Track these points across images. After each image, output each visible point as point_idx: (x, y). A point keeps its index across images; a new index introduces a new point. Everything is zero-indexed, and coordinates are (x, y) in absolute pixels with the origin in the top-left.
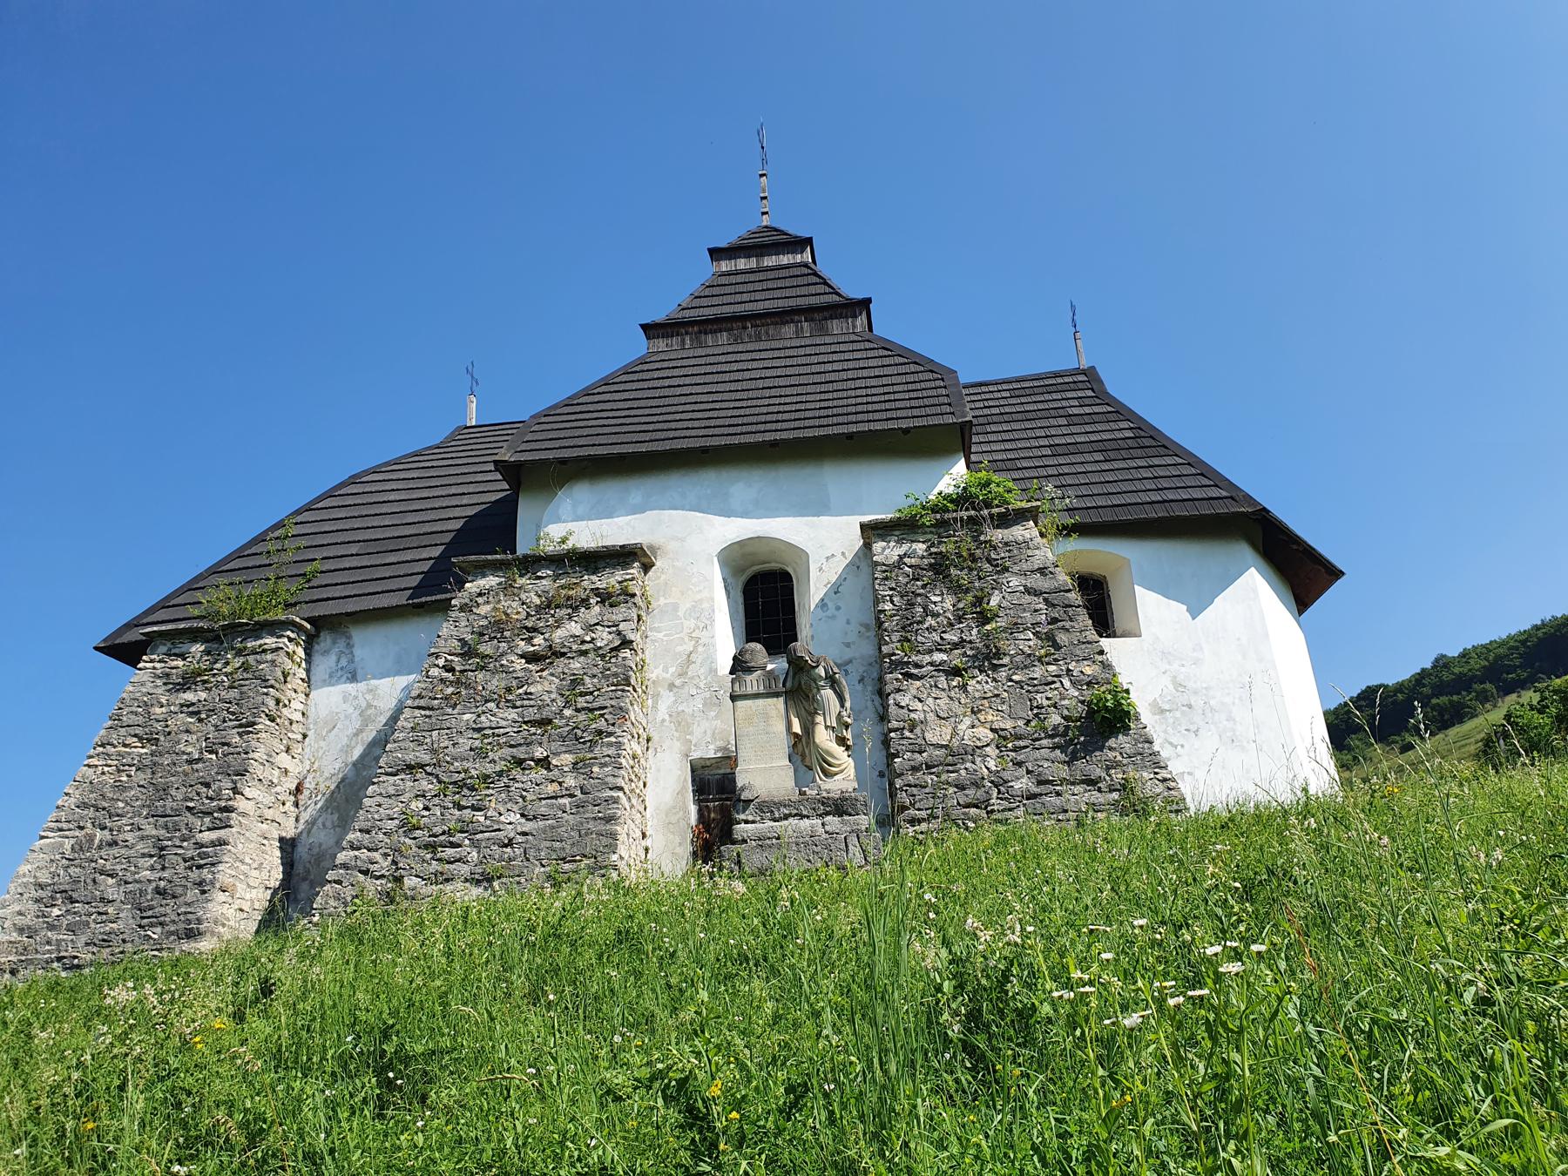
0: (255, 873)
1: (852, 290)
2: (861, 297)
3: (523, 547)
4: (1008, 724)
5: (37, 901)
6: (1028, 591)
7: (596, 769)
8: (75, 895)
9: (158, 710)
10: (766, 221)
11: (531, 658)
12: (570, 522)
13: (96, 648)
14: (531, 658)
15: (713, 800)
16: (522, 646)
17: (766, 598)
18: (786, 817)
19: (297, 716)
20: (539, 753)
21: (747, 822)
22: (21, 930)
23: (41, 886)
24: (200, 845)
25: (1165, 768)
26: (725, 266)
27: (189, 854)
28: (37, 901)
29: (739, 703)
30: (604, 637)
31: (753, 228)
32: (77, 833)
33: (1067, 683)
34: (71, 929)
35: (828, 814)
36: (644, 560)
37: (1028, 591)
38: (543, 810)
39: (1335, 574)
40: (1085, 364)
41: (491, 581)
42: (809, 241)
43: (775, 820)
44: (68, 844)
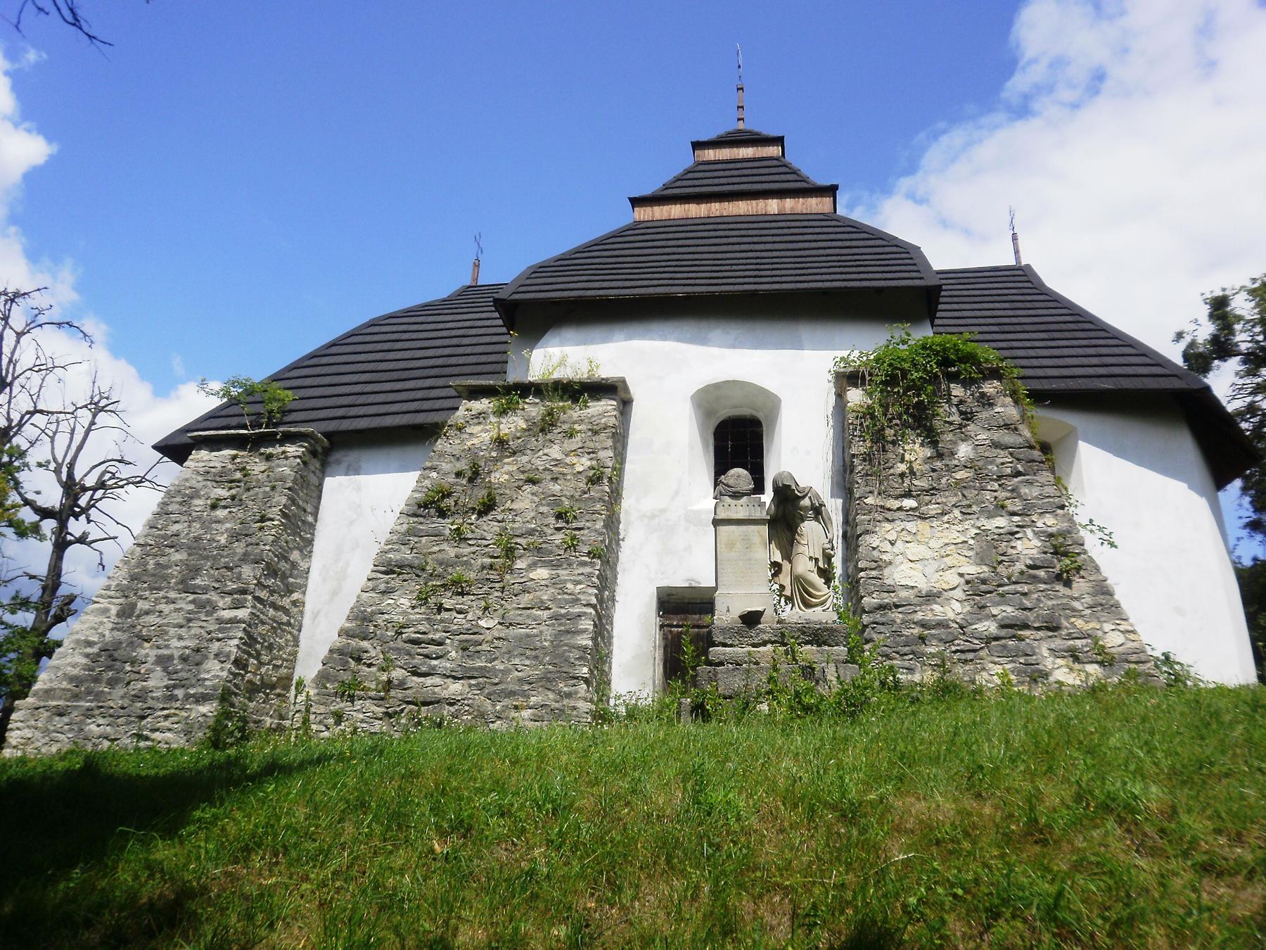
2: (828, 183)
3: (513, 377)
5: (87, 656)
6: (996, 445)
7: (570, 586)
8: (116, 654)
10: (741, 126)
12: (557, 356)
13: (155, 447)
15: (677, 626)
17: (738, 440)
19: (310, 519)
21: (725, 645)
23: (89, 644)
24: (220, 621)
26: (711, 154)
27: (212, 628)
28: (87, 656)
31: (731, 129)
32: (121, 600)
35: (807, 643)
36: (623, 395)
37: (996, 445)
38: (519, 619)
40: (1023, 263)
41: (483, 404)
42: (779, 141)
43: (754, 645)
44: (114, 610)
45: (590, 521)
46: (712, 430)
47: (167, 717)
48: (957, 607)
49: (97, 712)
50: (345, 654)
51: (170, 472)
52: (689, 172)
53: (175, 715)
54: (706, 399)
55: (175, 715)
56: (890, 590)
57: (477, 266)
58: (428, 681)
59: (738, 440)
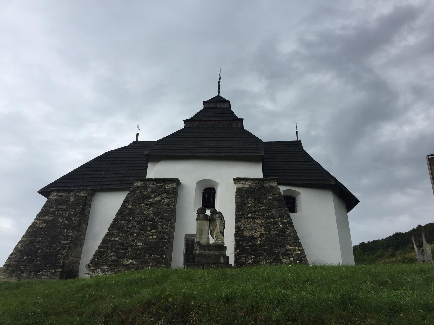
0: (73, 253)
1: (239, 116)
4: (264, 232)
9: (53, 209)
11: (147, 204)
14: (147, 204)
16: (146, 202)
18: (206, 250)
19: (87, 214)
20: (149, 228)
22: (16, 261)
24: (61, 244)
25: (302, 247)
29: (199, 221)
30: (166, 201)
33: (280, 223)
34: (28, 262)
35: (216, 250)
39: (359, 202)
42: (229, 102)
45: (169, 215)
46: (202, 191)
47: (46, 272)
48: (259, 242)
49: (25, 271)
50: (99, 253)
51: (43, 200)
52: (201, 111)
53: (48, 271)
54: (200, 183)
55: (48, 271)
56: (244, 236)
57: (138, 134)
58: (123, 260)
59: (208, 195)
